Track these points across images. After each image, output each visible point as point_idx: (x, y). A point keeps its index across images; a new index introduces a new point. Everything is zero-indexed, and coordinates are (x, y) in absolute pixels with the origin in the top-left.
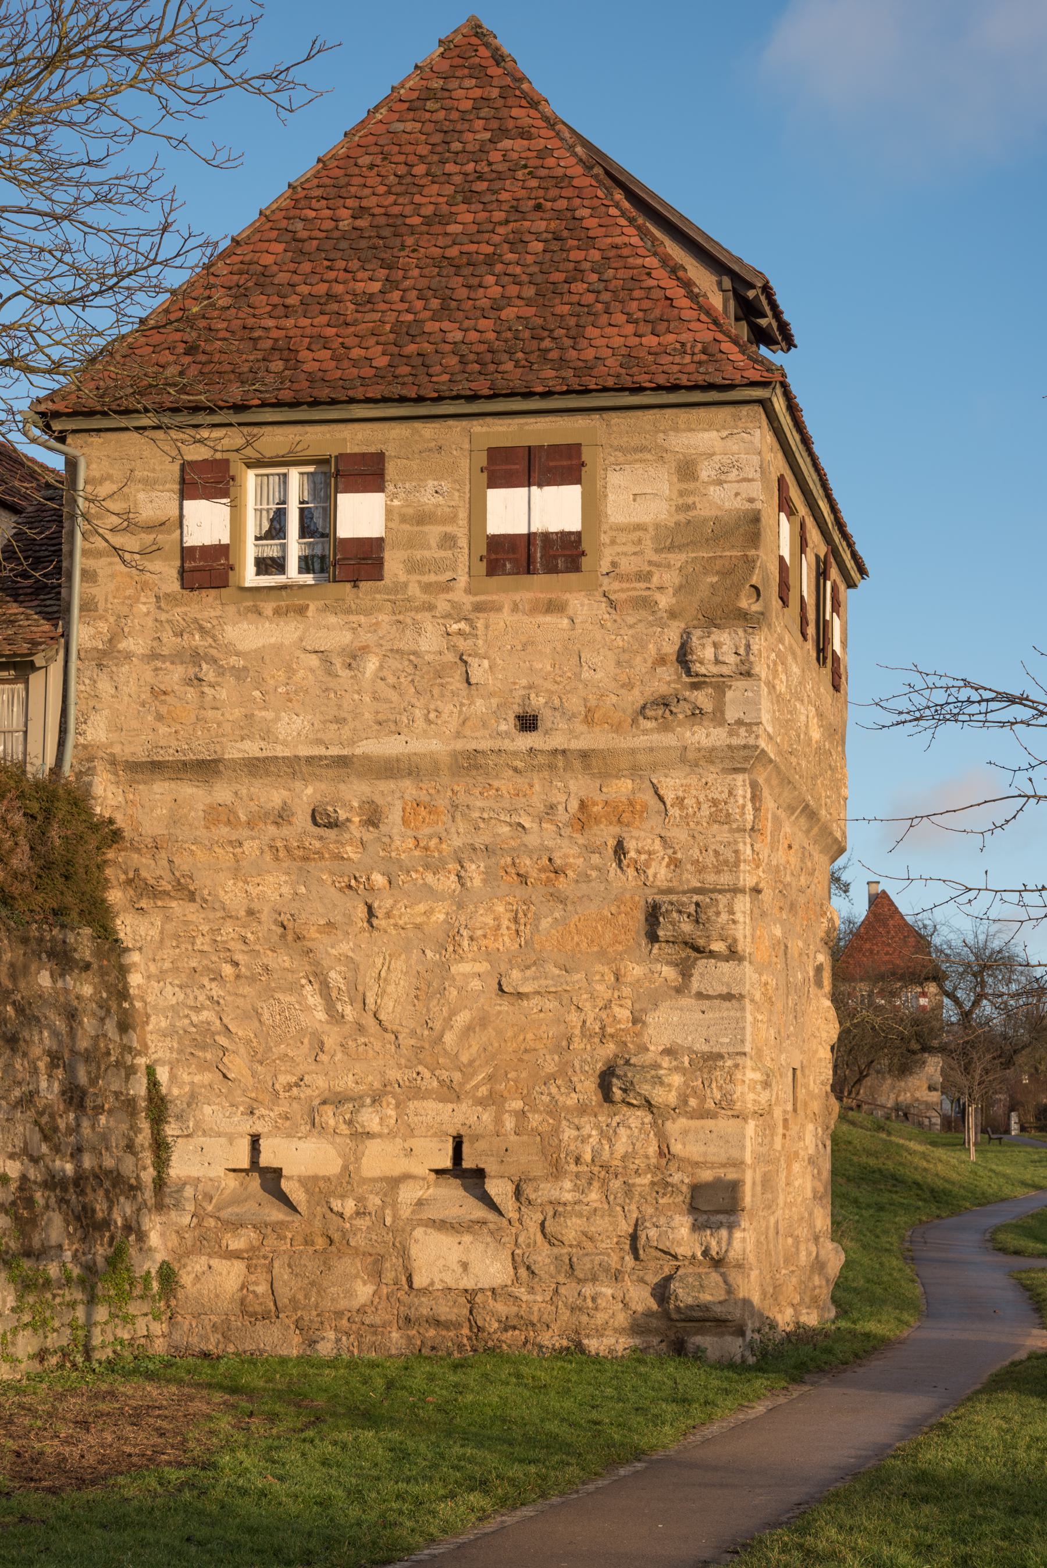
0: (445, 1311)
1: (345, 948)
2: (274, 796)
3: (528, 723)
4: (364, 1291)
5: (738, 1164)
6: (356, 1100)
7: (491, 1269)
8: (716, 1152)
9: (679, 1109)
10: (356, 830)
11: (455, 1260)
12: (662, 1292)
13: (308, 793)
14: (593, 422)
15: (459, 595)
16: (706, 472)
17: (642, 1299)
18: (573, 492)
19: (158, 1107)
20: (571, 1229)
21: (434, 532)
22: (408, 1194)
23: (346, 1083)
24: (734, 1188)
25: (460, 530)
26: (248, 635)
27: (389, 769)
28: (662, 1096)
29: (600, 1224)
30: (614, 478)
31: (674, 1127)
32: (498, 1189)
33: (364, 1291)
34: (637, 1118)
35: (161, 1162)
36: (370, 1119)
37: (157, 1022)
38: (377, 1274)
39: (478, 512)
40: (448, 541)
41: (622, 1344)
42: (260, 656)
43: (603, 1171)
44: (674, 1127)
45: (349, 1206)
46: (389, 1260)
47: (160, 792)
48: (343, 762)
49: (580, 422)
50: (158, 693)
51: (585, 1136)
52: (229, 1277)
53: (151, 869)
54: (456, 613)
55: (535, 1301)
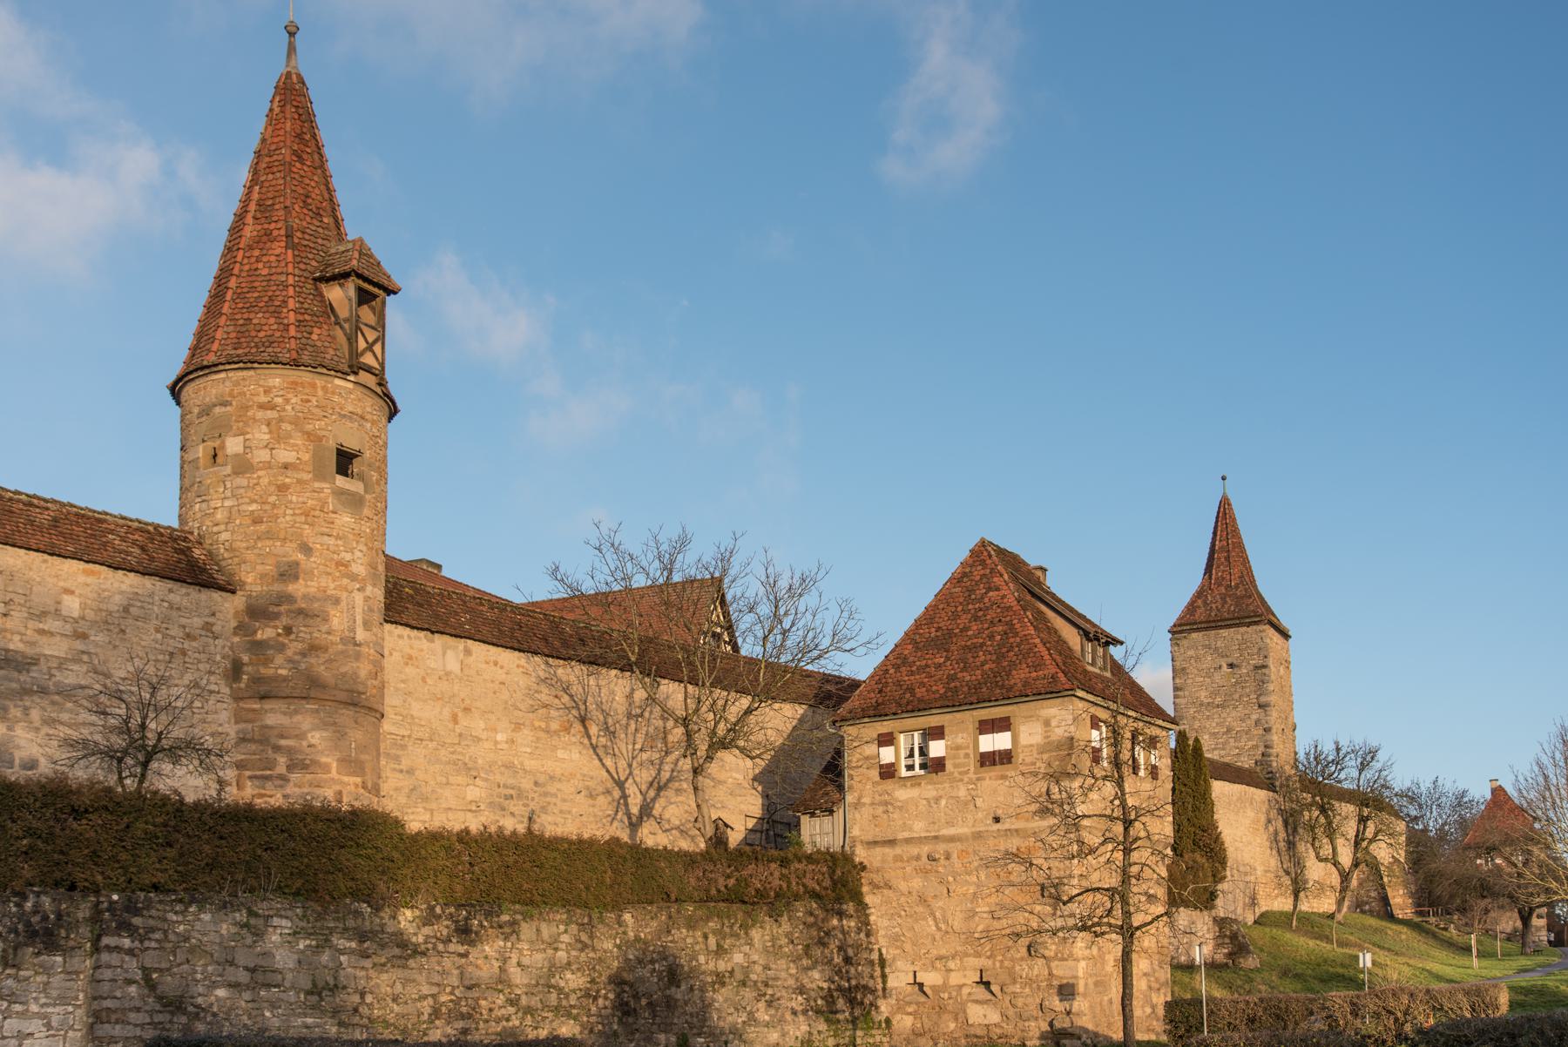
0: (979, 1032)
1: (941, 904)
2: (915, 851)
3: (997, 820)
4: (952, 1026)
5: (1076, 977)
6: (946, 958)
7: (994, 1017)
8: (1068, 973)
9: (1055, 958)
10: (942, 861)
11: (982, 1015)
12: (1051, 1024)
13: (926, 849)
14: (1014, 707)
15: (972, 775)
16: (1054, 723)
17: (1045, 1027)
18: (1008, 734)
19: (882, 962)
20: (1020, 1002)
21: (962, 753)
22: (965, 991)
23: (943, 952)
24: (1073, 986)
25: (971, 751)
26: (902, 794)
27: (952, 839)
28: (1047, 953)
29: (1030, 1000)
30: (1022, 728)
31: (1053, 965)
32: (994, 988)
33: (952, 1026)
34: (1041, 961)
35: (884, 982)
36: (951, 965)
37: (882, 932)
38: (956, 1019)
39: (976, 744)
40: (967, 755)
41: (1038, 1043)
42: (906, 802)
43: (1030, 981)
44: (1053, 965)
45: (946, 996)
46: (960, 1014)
47: (878, 850)
48: (936, 837)
49: (1010, 708)
50: (875, 817)
51: (1023, 969)
52: (908, 1021)
53: (877, 878)
54: (971, 782)
55: (1009, 1028)
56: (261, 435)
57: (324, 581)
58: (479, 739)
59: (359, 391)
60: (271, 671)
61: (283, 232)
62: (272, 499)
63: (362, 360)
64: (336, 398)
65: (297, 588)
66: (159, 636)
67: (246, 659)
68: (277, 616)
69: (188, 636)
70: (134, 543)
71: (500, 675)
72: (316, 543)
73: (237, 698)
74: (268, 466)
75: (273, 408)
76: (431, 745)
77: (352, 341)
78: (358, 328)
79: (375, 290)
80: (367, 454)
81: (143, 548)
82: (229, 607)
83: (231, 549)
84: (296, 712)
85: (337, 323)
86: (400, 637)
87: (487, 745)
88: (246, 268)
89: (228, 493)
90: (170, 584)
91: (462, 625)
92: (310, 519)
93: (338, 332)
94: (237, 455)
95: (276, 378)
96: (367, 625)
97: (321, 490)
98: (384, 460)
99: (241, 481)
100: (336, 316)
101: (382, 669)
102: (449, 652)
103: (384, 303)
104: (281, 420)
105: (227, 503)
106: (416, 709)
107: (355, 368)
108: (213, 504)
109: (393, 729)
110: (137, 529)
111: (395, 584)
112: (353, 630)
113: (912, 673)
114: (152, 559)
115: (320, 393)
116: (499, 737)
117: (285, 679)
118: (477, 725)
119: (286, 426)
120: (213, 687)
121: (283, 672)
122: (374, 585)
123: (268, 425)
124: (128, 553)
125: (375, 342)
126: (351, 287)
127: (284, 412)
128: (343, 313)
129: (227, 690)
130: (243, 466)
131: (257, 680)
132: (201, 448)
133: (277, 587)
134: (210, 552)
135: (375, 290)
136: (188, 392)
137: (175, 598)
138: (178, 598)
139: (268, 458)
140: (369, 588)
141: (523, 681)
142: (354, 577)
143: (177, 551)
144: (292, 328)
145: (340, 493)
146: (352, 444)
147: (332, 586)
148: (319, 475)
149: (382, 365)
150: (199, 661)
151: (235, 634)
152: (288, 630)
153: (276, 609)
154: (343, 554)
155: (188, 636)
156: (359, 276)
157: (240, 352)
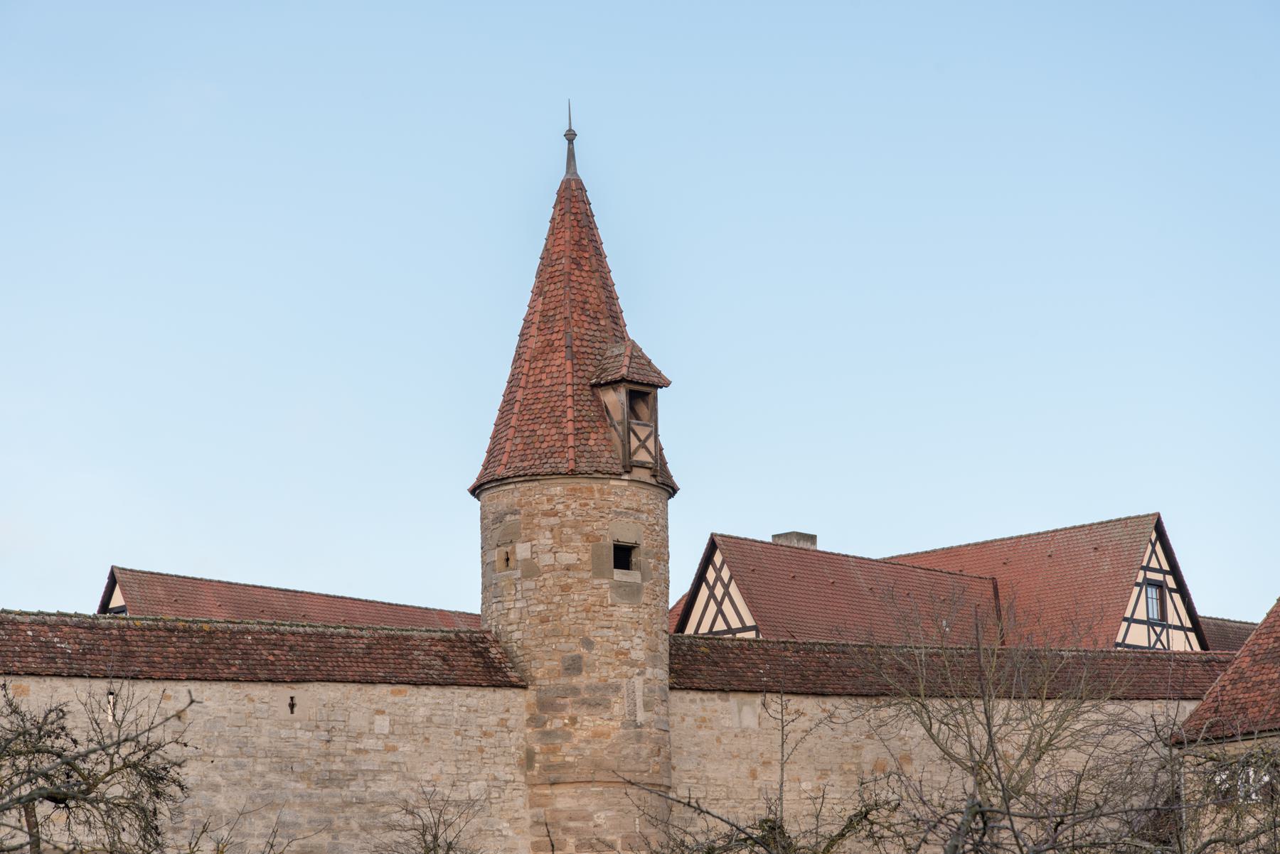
56: (545, 540)
59: (634, 487)
60: (559, 759)
62: (557, 599)
64: (612, 498)
65: (580, 681)
66: (459, 738)
67: (537, 748)
68: (563, 707)
69: (485, 734)
74: (552, 568)
75: (556, 515)
77: (626, 443)
78: (630, 429)
80: (644, 544)
81: (444, 659)
84: (583, 795)
86: (692, 701)
92: (590, 615)
93: (614, 434)
94: (525, 560)
95: (557, 488)
96: (647, 706)
97: (599, 587)
99: (530, 584)
100: (611, 419)
102: (746, 709)
103: (655, 398)
104: (562, 525)
105: (519, 605)
106: (711, 769)
108: (507, 605)
112: (633, 713)
113: (1248, 690)
114: (452, 668)
115: (597, 495)
117: (571, 765)
119: (567, 531)
123: (552, 530)
125: (648, 438)
129: (522, 778)
130: (531, 570)
131: (548, 767)
134: (505, 649)
135: (643, 390)
139: (551, 561)
140: (649, 670)
142: (633, 664)
143: (474, 654)
144: (571, 438)
146: (627, 538)
147: (612, 674)
148: (598, 573)
150: (496, 756)
151: (528, 726)
152: (573, 720)
153: (562, 701)
155: (485, 734)
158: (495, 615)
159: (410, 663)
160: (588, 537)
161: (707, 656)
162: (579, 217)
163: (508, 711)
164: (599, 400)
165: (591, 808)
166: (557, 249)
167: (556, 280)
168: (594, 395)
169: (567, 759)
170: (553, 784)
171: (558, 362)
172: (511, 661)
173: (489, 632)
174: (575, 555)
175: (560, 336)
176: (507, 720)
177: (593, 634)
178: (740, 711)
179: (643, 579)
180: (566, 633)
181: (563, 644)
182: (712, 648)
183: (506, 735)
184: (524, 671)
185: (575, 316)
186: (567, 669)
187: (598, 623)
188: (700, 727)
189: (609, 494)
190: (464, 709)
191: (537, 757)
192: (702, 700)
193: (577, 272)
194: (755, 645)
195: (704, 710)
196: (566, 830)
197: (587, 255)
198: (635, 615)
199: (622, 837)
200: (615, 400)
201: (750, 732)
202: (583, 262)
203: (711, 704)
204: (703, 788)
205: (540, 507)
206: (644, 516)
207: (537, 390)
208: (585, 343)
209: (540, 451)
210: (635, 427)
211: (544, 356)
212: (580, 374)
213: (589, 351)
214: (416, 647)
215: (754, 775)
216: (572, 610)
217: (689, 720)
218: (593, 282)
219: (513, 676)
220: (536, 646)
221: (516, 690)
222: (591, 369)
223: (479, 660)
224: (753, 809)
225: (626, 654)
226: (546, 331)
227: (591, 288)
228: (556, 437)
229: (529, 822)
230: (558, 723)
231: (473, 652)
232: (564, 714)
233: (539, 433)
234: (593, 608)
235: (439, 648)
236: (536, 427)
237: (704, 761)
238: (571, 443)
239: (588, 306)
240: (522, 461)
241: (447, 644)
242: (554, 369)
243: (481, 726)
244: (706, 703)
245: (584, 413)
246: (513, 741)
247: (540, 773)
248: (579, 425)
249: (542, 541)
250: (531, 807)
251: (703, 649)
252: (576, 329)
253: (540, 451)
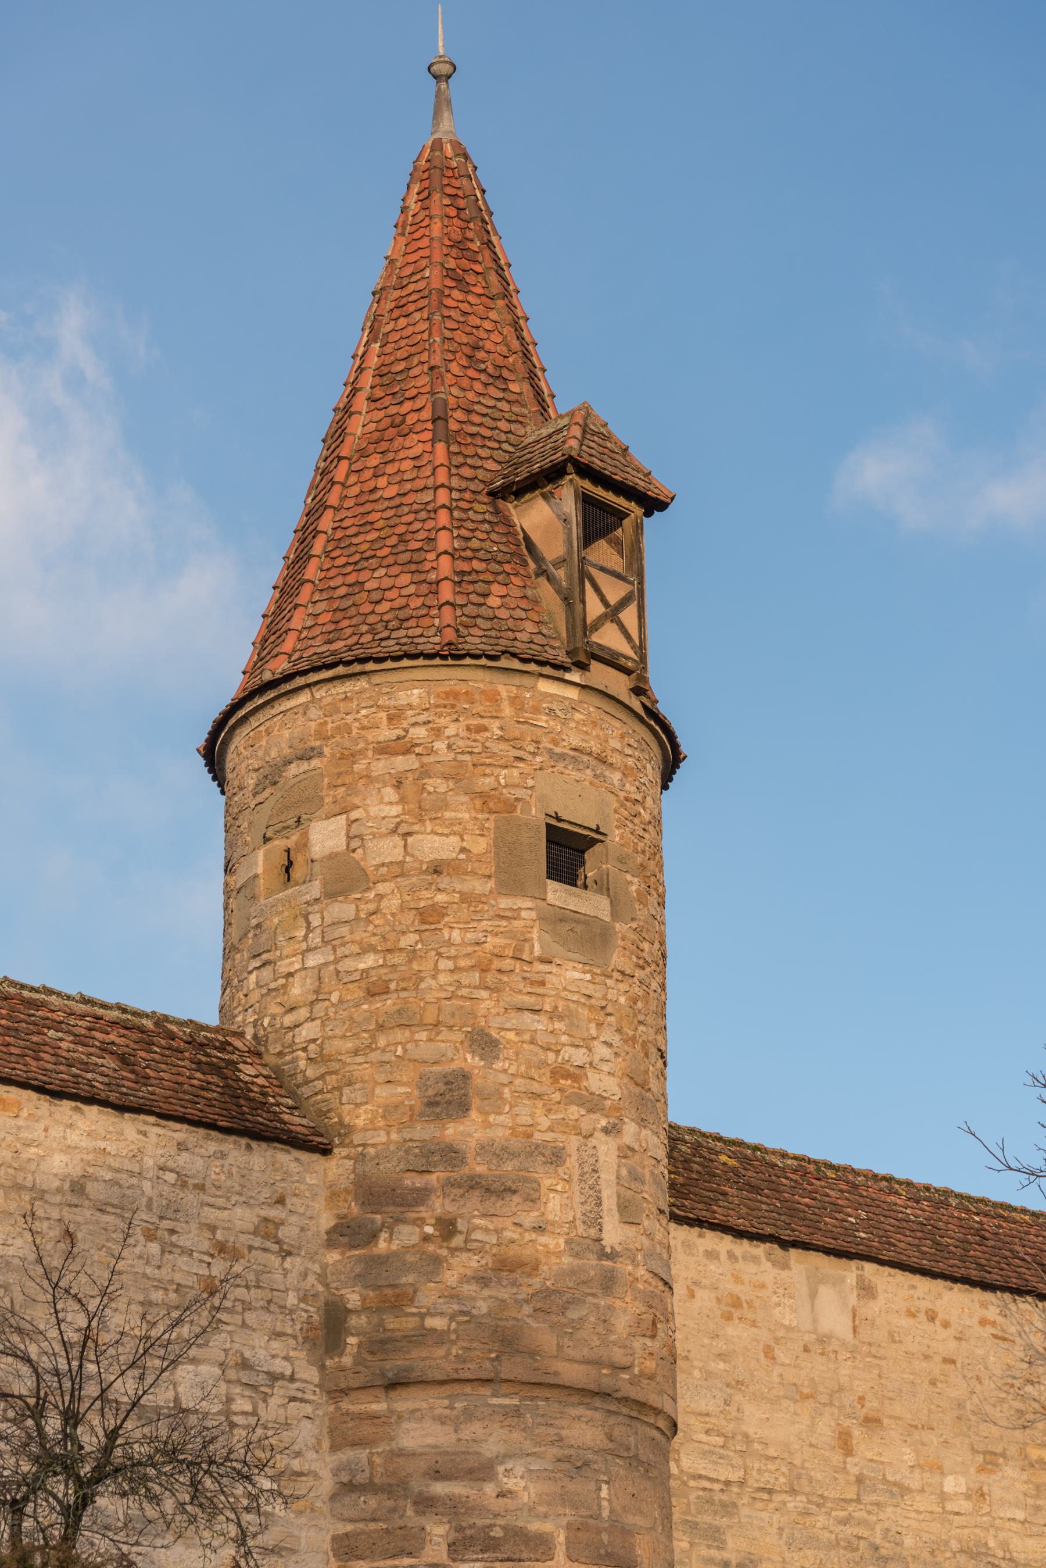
56: (383, 807)
57: (526, 1113)
58: (905, 1490)
59: (592, 705)
61: (426, 414)
62: (408, 940)
63: (595, 638)
64: (542, 721)
65: (467, 1131)
66: (154, 1248)
67: (353, 1298)
68: (421, 1196)
69: (222, 1248)
70: (105, 1049)
71: (944, 1343)
72: (506, 1028)
73: (337, 1393)
74: (398, 871)
75: (407, 751)
76: (795, 1503)
77: (572, 601)
78: (584, 575)
79: (621, 502)
80: (616, 836)
81: (124, 1060)
82: (314, 1187)
83: (321, 1059)
84: (469, 1415)
85: (542, 572)
86: (711, 1255)
87: (922, 1503)
88: (355, 490)
89: (315, 939)
90: (181, 1132)
91: (850, 1231)
92: (490, 978)
93: (545, 591)
94: (332, 856)
95: (413, 690)
96: (627, 1212)
97: (514, 915)
98: (656, 850)
101: (669, 1317)
102: (826, 1293)
103: (639, 528)
104: (424, 772)
105: (312, 961)
106: (754, 1419)
107: (584, 656)
108: (283, 967)
109: (702, 1467)
110: (114, 1023)
111: (697, 1147)
112: (595, 1221)
114: (143, 1080)
115: (507, 711)
116: (951, 1484)
117: (440, 1338)
118: (897, 1457)
119: (437, 785)
120: (280, 1366)
121: (436, 1323)
122: (642, 1122)
123: (398, 785)
124: (86, 1067)
125: (624, 603)
126: (567, 495)
127: (437, 760)
128: (552, 548)
129: (312, 1374)
132: (261, 854)
133: (423, 1132)
136: (243, 753)
137: (191, 1163)
138: (199, 1163)
139: (398, 854)
140: (630, 1129)
141: (997, 1359)
142: (593, 1103)
145: (557, 919)
146: (580, 812)
147: (545, 1122)
148: (510, 882)
149: (641, 650)
150: (247, 1307)
151: (331, 1244)
152: (447, 1227)
153: (419, 1181)
154: (567, 1052)
156: (585, 471)
157: (339, 645)
158: (254, 997)
159: (36, 1051)
160: (485, 800)
161: (734, 1171)
162: (462, 203)
163: (281, 1201)
164: (509, 524)
165: (491, 1448)
166: (412, 258)
167: (411, 308)
168: (497, 512)
169: (431, 1322)
170: (393, 1385)
171: (417, 450)
172: (292, 1095)
173: (241, 1035)
174: (454, 840)
175: (419, 403)
176: (279, 1224)
177: (495, 1023)
178: (813, 1295)
179: (615, 914)
180: (430, 1018)
181: (422, 1044)
182: (745, 1161)
183: (274, 1261)
184: (325, 1114)
185: (454, 367)
186: (431, 1104)
187: (509, 998)
188: (729, 1317)
189: (536, 710)
190: (171, 1177)
191: (353, 1321)
192: (731, 1255)
193: (456, 294)
194: (830, 1174)
195: (738, 1280)
196: (426, 1504)
197: (478, 268)
198: (597, 992)
199: (569, 1527)
200: (546, 519)
201: (835, 1345)
202: (471, 278)
203: (752, 1268)
204: (737, 1460)
205: (370, 736)
206: (616, 777)
207: (368, 507)
208: (476, 419)
209: (371, 619)
210: (594, 572)
211: (384, 446)
212: (466, 472)
213: (487, 433)
214: (57, 1025)
215: (845, 1443)
216: (444, 964)
217: (705, 1298)
218: (493, 315)
219: (296, 1122)
220: (356, 1052)
221: (305, 1156)
222: (491, 465)
223: (215, 1079)
224: (844, 1522)
225: (576, 1078)
226: (387, 401)
227: (488, 325)
228: (412, 589)
229: (327, 1485)
230: (407, 1235)
231: (199, 1063)
232: (423, 1212)
233: (368, 586)
234: (497, 964)
235: (112, 1037)
236: (364, 576)
237: (738, 1397)
238: (447, 592)
239: (481, 355)
240: (330, 642)
241: (136, 1035)
242: (407, 465)
243: (213, 1229)
244: (740, 1265)
245: (475, 544)
246: (293, 1278)
247: (358, 1361)
248: (465, 567)
249: (374, 811)
250: (334, 1448)
251: (723, 1158)
252: (455, 391)
253: (371, 619)
